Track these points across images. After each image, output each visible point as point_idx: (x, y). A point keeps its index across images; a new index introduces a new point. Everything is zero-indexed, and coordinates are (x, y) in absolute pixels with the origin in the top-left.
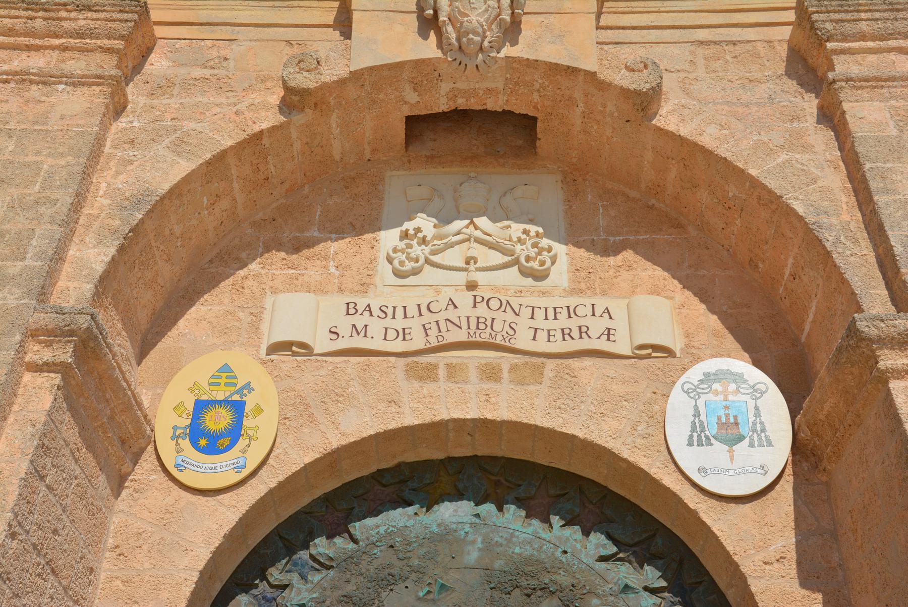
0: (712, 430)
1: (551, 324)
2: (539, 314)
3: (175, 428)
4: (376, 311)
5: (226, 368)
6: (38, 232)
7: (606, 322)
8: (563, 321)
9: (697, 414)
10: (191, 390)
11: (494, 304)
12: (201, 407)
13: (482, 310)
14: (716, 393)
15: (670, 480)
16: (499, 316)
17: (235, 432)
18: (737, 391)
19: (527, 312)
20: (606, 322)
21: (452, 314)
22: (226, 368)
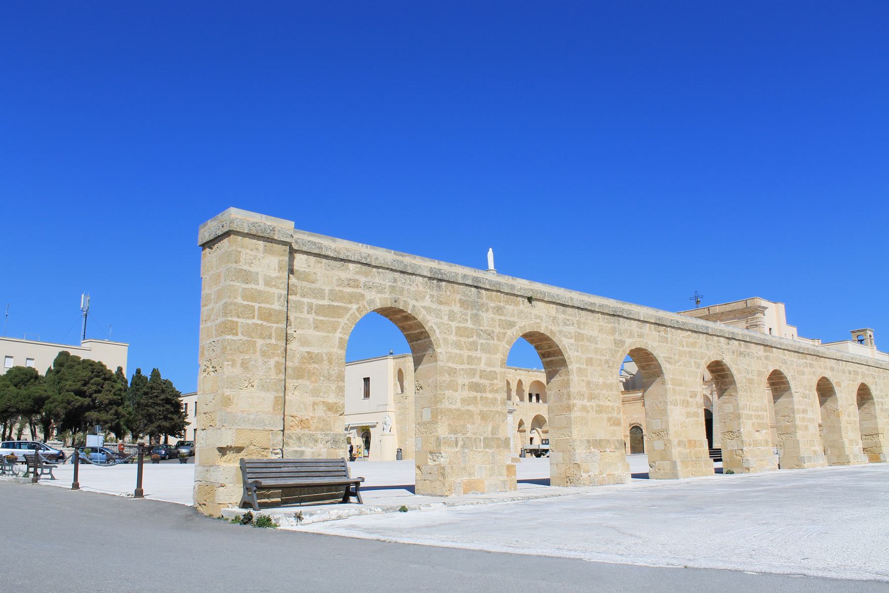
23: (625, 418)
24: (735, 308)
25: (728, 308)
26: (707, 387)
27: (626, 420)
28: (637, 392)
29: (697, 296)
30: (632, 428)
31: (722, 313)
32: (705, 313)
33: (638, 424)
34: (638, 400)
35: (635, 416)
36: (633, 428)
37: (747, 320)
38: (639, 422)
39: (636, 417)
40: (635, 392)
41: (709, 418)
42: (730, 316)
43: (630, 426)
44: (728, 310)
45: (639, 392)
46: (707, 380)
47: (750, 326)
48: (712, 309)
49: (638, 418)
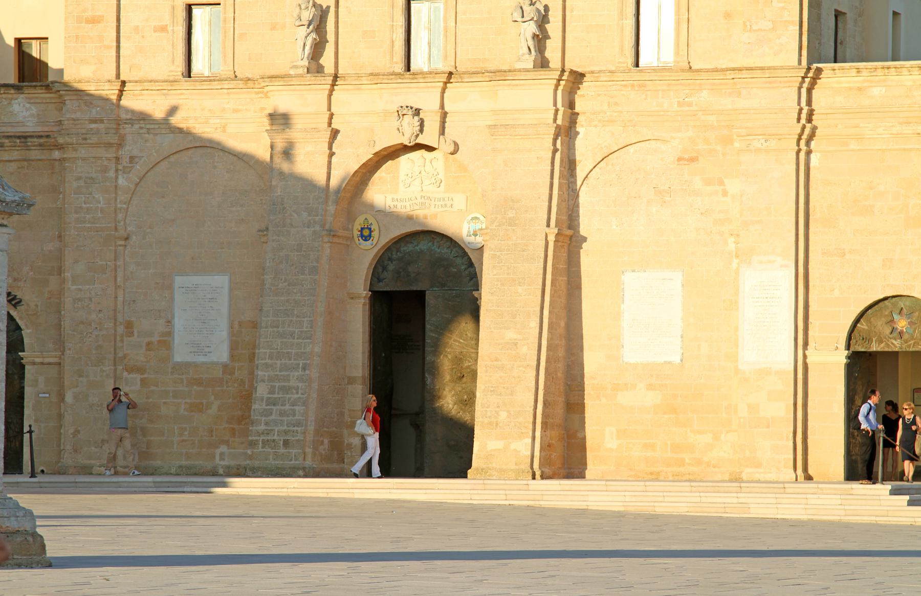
0: (472, 233)
1: (437, 203)
2: (436, 199)
3: (358, 235)
4: (399, 200)
5: (366, 219)
6: (320, 208)
7: (451, 202)
8: (442, 203)
9: (469, 229)
10: (360, 225)
11: (426, 198)
12: (362, 229)
13: (423, 200)
14: (473, 223)
16: (427, 201)
17: (370, 236)
18: (478, 223)
19: (433, 200)
20: (451, 202)
21: (416, 201)
22: (366, 219)
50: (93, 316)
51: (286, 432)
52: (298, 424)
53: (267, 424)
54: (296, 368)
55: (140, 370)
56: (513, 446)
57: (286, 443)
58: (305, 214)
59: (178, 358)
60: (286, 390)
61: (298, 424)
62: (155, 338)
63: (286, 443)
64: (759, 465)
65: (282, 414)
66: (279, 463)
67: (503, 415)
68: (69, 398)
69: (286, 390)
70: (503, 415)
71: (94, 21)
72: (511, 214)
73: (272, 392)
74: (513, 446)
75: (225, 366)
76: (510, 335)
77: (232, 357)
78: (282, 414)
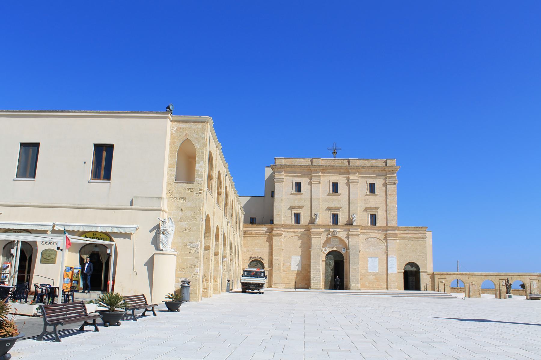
15: (341, 252)
23: (245, 250)
24: (375, 165)
25: (368, 163)
26: (342, 230)
27: (247, 253)
28: (262, 226)
29: (336, 148)
30: (251, 262)
31: (364, 167)
32: (344, 164)
33: (259, 258)
34: (261, 235)
35: (257, 250)
36: (252, 261)
37: (386, 177)
38: (262, 257)
39: (258, 251)
40: (259, 226)
41: (338, 259)
42: (370, 171)
43: (251, 258)
44: (367, 165)
45: (265, 227)
46: (341, 224)
47: (389, 183)
48: (351, 162)
49: (259, 252)
50: (278, 262)
51: (317, 282)
52: (319, 281)
53: (313, 281)
54: (318, 272)
55: (286, 271)
56: (357, 285)
57: (317, 284)
58: (318, 247)
59: (292, 270)
60: (316, 275)
61: (319, 281)
62: (288, 266)
63: (317, 284)
64: (391, 288)
65: (316, 279)
66: (316, 287)
67: (354, 280)
68: (273, 276)
69: (316, 275)
70: (354, 280)
71: (279, 215)
72: (353, 248)
73: (314, 276)
74: (357, 285)
75: (300, 271)
76: (355, 267)
77: (302, 270)
78: (316, 279)
